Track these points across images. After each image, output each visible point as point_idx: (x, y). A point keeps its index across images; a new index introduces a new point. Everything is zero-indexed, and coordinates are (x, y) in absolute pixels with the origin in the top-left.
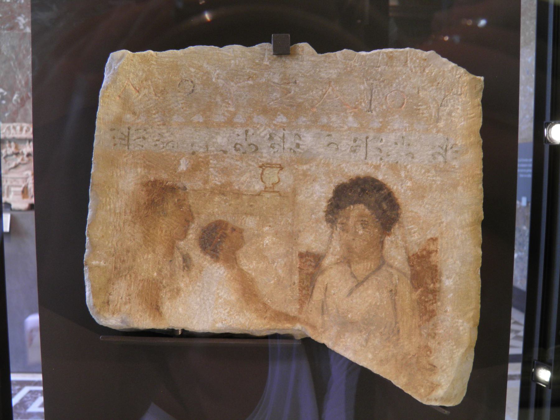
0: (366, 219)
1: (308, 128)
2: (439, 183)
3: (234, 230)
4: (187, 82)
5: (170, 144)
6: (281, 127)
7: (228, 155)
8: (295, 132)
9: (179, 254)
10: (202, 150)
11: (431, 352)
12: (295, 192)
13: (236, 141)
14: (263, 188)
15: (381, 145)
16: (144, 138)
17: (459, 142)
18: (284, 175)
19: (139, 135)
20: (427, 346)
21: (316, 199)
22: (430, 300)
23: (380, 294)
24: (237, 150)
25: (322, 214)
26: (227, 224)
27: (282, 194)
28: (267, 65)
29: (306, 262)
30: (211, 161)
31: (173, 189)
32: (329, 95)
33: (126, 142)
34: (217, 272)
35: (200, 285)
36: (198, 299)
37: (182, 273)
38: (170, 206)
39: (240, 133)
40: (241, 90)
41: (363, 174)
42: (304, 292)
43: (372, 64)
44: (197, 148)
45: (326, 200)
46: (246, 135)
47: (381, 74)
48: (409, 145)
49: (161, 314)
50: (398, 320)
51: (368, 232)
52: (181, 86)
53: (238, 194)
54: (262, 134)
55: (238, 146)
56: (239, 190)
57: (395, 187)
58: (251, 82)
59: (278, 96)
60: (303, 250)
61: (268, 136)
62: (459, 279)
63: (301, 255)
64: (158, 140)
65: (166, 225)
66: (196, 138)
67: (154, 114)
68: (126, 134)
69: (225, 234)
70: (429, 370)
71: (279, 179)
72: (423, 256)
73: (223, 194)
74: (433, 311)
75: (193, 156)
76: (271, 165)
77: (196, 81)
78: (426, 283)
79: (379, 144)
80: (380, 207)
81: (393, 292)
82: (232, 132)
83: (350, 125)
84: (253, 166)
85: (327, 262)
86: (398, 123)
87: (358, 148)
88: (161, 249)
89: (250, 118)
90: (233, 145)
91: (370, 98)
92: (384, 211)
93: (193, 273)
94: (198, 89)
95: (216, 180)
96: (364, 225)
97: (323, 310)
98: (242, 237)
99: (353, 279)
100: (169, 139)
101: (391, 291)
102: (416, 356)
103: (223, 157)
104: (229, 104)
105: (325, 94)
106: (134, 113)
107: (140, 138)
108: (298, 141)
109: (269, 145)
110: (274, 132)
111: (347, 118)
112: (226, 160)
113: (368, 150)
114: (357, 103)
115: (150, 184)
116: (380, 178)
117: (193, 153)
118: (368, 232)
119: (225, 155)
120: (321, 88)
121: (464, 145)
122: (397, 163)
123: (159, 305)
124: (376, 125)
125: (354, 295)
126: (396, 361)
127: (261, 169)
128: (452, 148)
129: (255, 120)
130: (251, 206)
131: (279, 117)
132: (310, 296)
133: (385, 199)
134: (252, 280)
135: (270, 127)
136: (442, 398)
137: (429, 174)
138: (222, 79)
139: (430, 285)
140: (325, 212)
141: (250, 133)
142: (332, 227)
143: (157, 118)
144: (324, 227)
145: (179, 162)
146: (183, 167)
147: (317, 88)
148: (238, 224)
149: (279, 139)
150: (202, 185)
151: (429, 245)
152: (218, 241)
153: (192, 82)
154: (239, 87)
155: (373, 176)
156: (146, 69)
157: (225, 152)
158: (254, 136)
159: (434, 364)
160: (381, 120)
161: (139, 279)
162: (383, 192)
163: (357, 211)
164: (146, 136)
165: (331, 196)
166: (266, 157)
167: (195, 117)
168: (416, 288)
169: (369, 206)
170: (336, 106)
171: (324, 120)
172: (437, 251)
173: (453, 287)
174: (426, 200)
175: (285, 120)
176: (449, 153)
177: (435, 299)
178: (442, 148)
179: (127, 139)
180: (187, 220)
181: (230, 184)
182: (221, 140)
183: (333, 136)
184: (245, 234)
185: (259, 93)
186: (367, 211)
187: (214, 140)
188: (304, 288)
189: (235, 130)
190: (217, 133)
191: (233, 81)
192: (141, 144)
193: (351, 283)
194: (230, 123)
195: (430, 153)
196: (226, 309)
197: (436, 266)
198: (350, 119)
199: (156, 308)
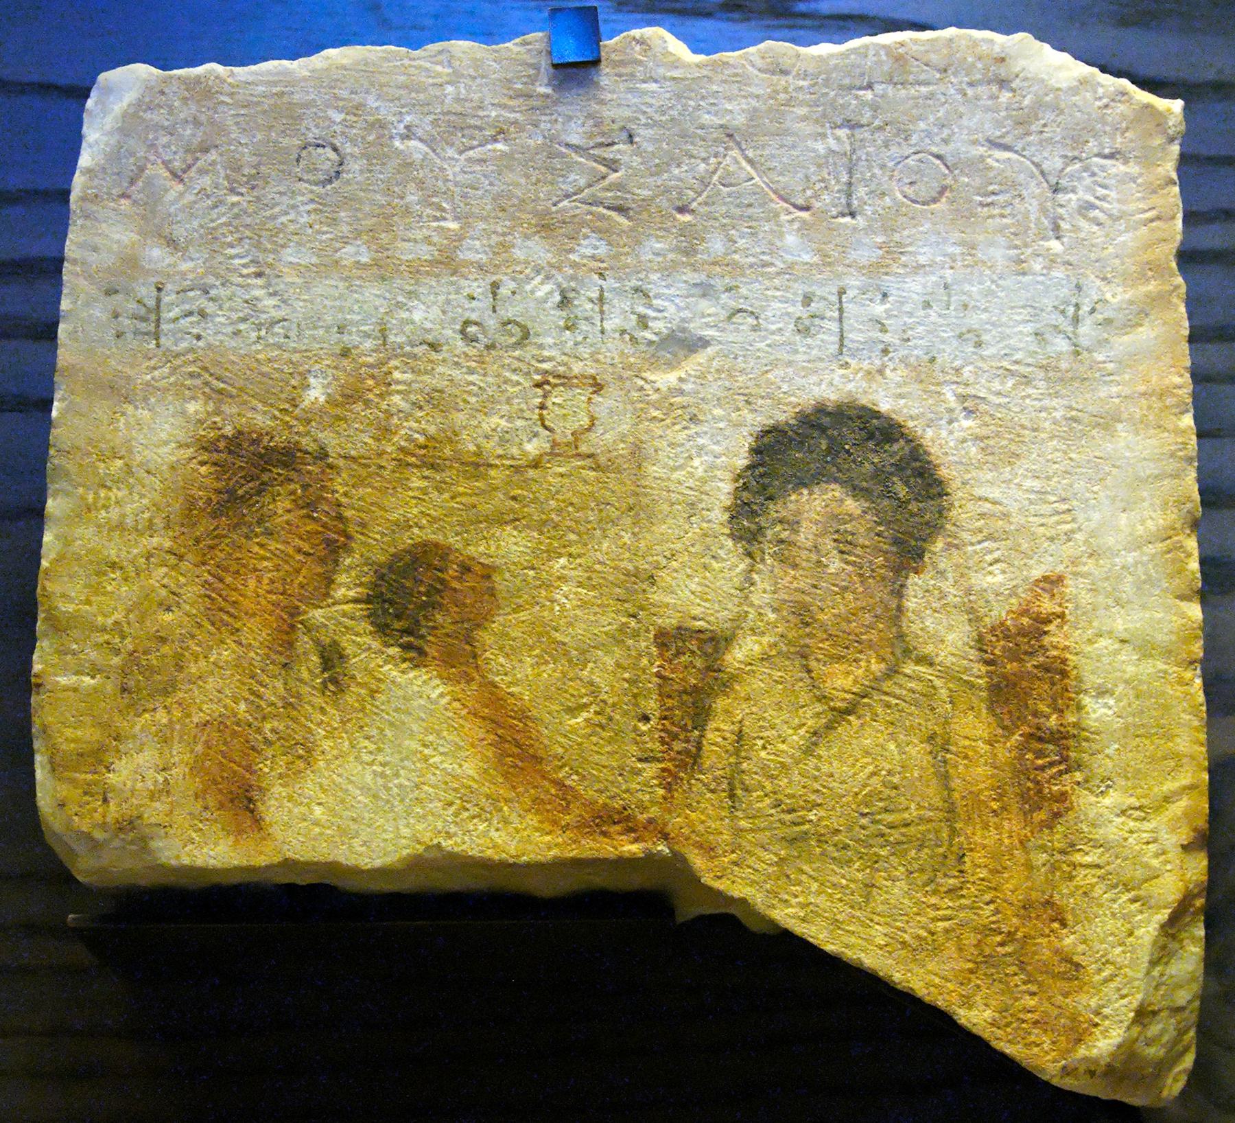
0: (849, 527)
1: (669, 270)
2: (1058, 415)
3: (466, 569)
4: (320, 150)
5: (277, 329)
6: (591, 270)
7: (444, 355)
8: (634, 283)
9: (310, 645)
10: (368, 344)
11: (1064, 924)
12: (638, 453)
13: (467, 315)
14: (547, 446)
15: (886, 311)
16: (202, 314)
17: (1117, 296)
18: (604, 404)
19: (187, 307)
20: (1048, 903)
21: (700, 472)
22: (1052, 764)
23: (898, 746)
24: (471, 340)
25: (719, 516)
26: (444, 552)
27: (602, 460)
28: (547, 96)
29: (679, 653)
30: (397, 375)
31: (288, 457)
32: (729, 174)
33: (152, 328)
34: (420, 691)
35: (375, 732)
36: (369, 778)
37: (319, 701)
38: (281, 507)
39: (477, 292)
40: (478, 168)
41: (833, 397)
42: (678, 746)
43: (847, 81)
44: (356, 339)
45: (729, 476)
46: (495, 294)
47: (875, 108)
48: (965, 306)
49: (257, 822)
50: (958, 826)
51: (853, 564)
52: (302, 163)
53: (477, 465)
54: (540, 294)
55: (472, 329)
56: (478, 454)
57: (930, 433)
58: (500, 146)
59: (582, 182)
60: (669, 621)
61: (558, 298)
62: (1137, 697)
63: (663, 639)
64: (244, 320)
65: (268, 559)
66: (351, 311)
67: (231, 246)
68: (151, 303)
69: (442, 581)
70: (1062, 976)
71: (593, 419)
72: (1022, 632)
73: (433, 466)
74: (1063, 797)
75: (345, 362)
76: (566, 380)
77: (348, 148)
78: (1035, 714)
79: (879, 309)
80: (889, 494)
81: (939, 743)
82: (451, 289)
83: (789, 258)
84: (518, 383)
85: (736, 656)
86: (930, 243)
87: (817, 321)
88: (256, 633)
89: (505, 247)
90: (458, 327)
91: (845, 178)
92: (902, 504)
93: (350, 699)
94: (354, 167)
95: (415, 427)
96: (845, 545)
97: (733, 790)
98: (492, 592)
99: (819, 708)
100: (277, 314)
101: (931, 738)
102: (1019, 935)
103: (432, 362)
104: (444, 210)
105: (714, 172)
106: (172, 243)
107: (191, 314)
108: (641, 310)
109: (562, 323)
110: (573, 284)
111: (781, 236)
112: (440, 369)
113: (846, 327)
114: (809, 193)
115: (222, 445)
116: (884, 407)
117: (345, 353)
118: (853, 564)
119: (434, 356)
120: (704, 155)
121: (1131, 302)
122: (933, 360)
123: (255, 794)
124: (864, 255)
125: (821, 751)
126: (960, 950)
127: (539, 391)
128: (1093, 311)
129: (518, 254)
130: (514, 498)
131: (584, 242)
132: (692, 759)
133: (899, 467)
134: (523, 716)
135: (559, 269)
136: (1110, 1071)
137: (1030, 391)
138: (421, 140)
139: (1048, 717)
140: (727, 509)
141: (504, 291)
142: (749, 554)
143: (239, 258)
144: (730, 560)
145: (304, 376)
146: (316, 393)
147: (692, 156)
148: (477, 550)
149: (589, 306)
150: (370, 441)
151: (1037, 597)
152: (423, 602)
153: (335, 149)
154: (469, 160)
155: (864, 401)
156: (203, 118)
157: (434, 346)
158: (518, 297)
159: (1076, 959)
160: (880, 239)
161: (196, 720)
162: (896, 447)
163: (816, 506)
164: (210, 308)
165: (742, 462)
166: (550, 359)
167: (349, 249)
168: (1004, 728)
169: (857, 491)
170: (750, 205)
171: (716, 245)
172: (1061, 616)
173: (1118, 724)
174: (1022, 466)
175: (603, 250)
176: (1086, 330)
177: (1065, 759)
178: (1063, 312)
179: (153, 317)
180: (333, 547)
181: (452, 437)
182: (421, 315)
183: (743, 291)
184: (497, 578)
185: (527, 176)
186: (852, 505)
187: (404, 315)
188: (675, 737)
189: (463, 282)
190: (411, 294)
191: (452, 145)
192: (195, 331)
193: (812, 716)
194: (448, 262)
195: (1029, 328)
196: (450, 804)
197: (1064, 661)
198: (791, 240)
199: (241, 803)
